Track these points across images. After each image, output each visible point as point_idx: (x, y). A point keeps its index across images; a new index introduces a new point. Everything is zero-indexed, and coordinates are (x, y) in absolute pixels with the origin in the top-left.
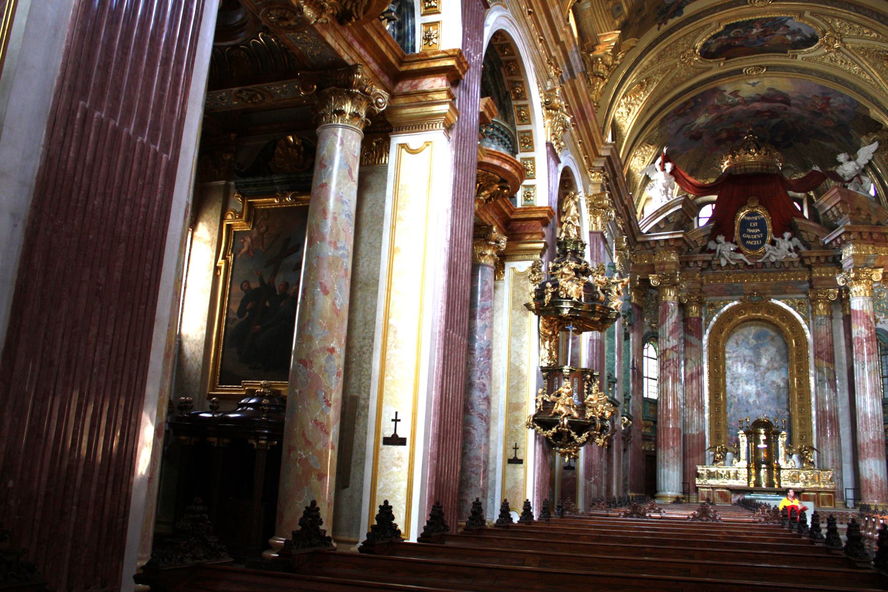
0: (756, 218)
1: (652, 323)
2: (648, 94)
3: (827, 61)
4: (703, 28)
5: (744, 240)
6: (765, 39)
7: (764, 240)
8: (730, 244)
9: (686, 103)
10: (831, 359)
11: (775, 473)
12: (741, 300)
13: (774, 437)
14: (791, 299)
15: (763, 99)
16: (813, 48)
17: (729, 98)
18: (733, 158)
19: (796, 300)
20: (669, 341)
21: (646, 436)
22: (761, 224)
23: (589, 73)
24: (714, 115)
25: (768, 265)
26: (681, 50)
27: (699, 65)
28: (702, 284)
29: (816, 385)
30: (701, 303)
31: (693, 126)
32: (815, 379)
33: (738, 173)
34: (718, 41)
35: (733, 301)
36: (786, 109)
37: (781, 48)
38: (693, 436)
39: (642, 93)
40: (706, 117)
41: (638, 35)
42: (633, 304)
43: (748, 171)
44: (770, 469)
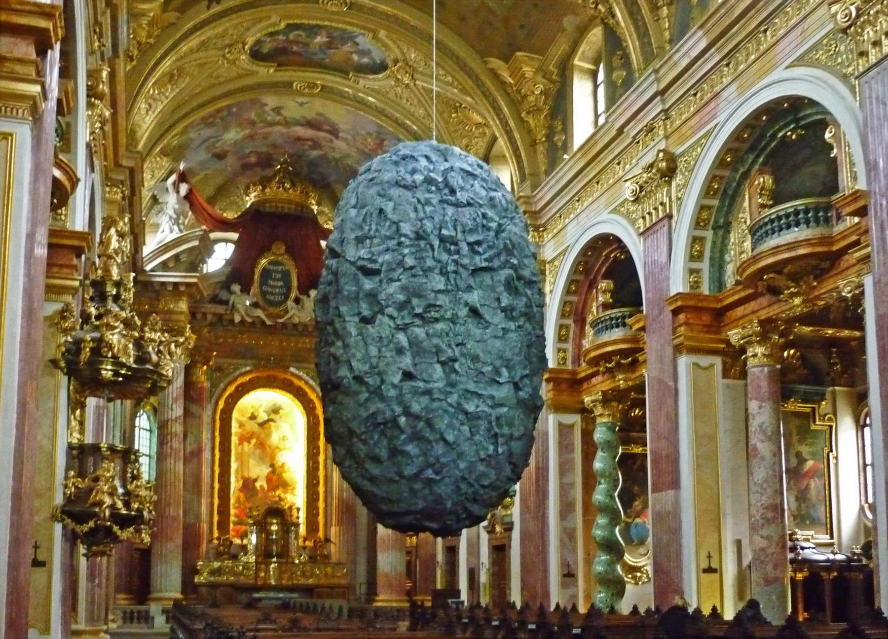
0: (280, 268)
2: (178, 90)
4: (260, 20)
5: (264, 294)
7: (287, 296)
9: (219, 111)
15: (310, 124)
17: (269, 115)
22: (286, 276)
25: (290, 327)
26: (227, 42)
27: (245, 66)
31: (218, 141)
33: (267, 210)
34: (275, 40)
36: (331, 141)
37: (342, 70)
43: (280, 210)
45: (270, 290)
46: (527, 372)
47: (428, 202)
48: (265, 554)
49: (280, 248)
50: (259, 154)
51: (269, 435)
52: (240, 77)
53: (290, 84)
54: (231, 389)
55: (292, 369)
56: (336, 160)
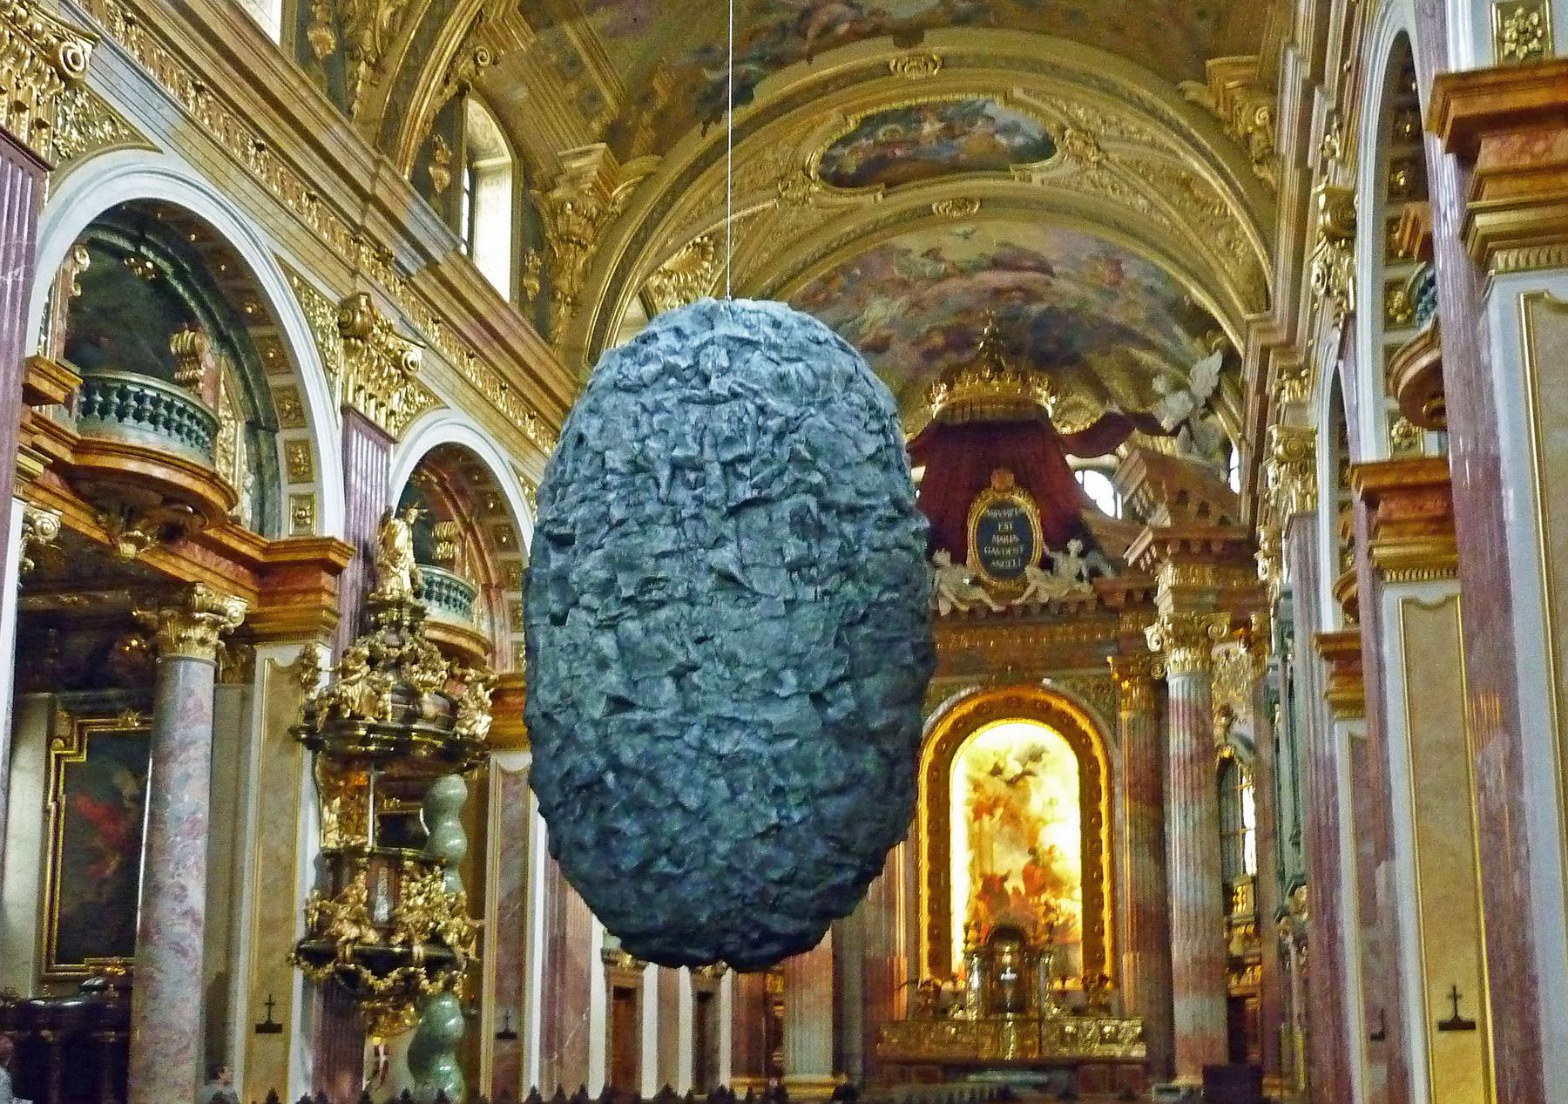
0: (1009, 513)
3: (1087, 186)
5: (986, 560)
6: (955, 143)
7: (1026, 558)
8: (959, 568)
15: (996, 264)
16: (1047, 163)
18: (950, 388)
22: (1021, 522)
23: (549, 235)
24: (903, 300)
25: (1035, 611)
26: (774, 173)
33: (959, 421)
35: (966, 685)
36: (1048, 284)
37: (993, 163)
39: (706, 264)
40: (886, 305)
41: (660, 148)
45: (995, 551)
46: (841, 671)
47: (659, 407)
48: (993, 1003)
49: (1002, 479)
50: (946, 331)
51: (1025, 799)
52: (830, 221)
53: (927, 211)
54: (1084, 724)
55: (1046, 681)
56: (1070, 311)
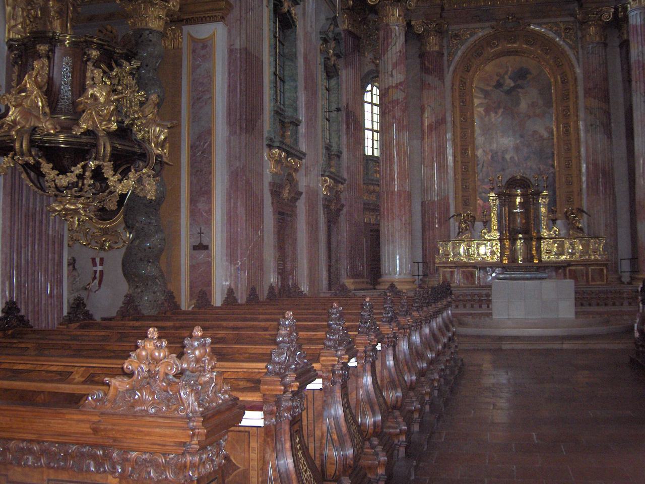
1: (376, 58)
10: (605, 97)
11: (534, 243)
12: (493, 28)
13: (533, 199)
14: (557, 24)
19: (561, 25)
20: (392, 76)
21: (369, 204)
28: (443, 9)
29: (587, 131)
30: (441, 33)
32: (586, 126)
35: (483, 28)
38: (433, 202)
42: (344, 30)
44: (528, 240)
